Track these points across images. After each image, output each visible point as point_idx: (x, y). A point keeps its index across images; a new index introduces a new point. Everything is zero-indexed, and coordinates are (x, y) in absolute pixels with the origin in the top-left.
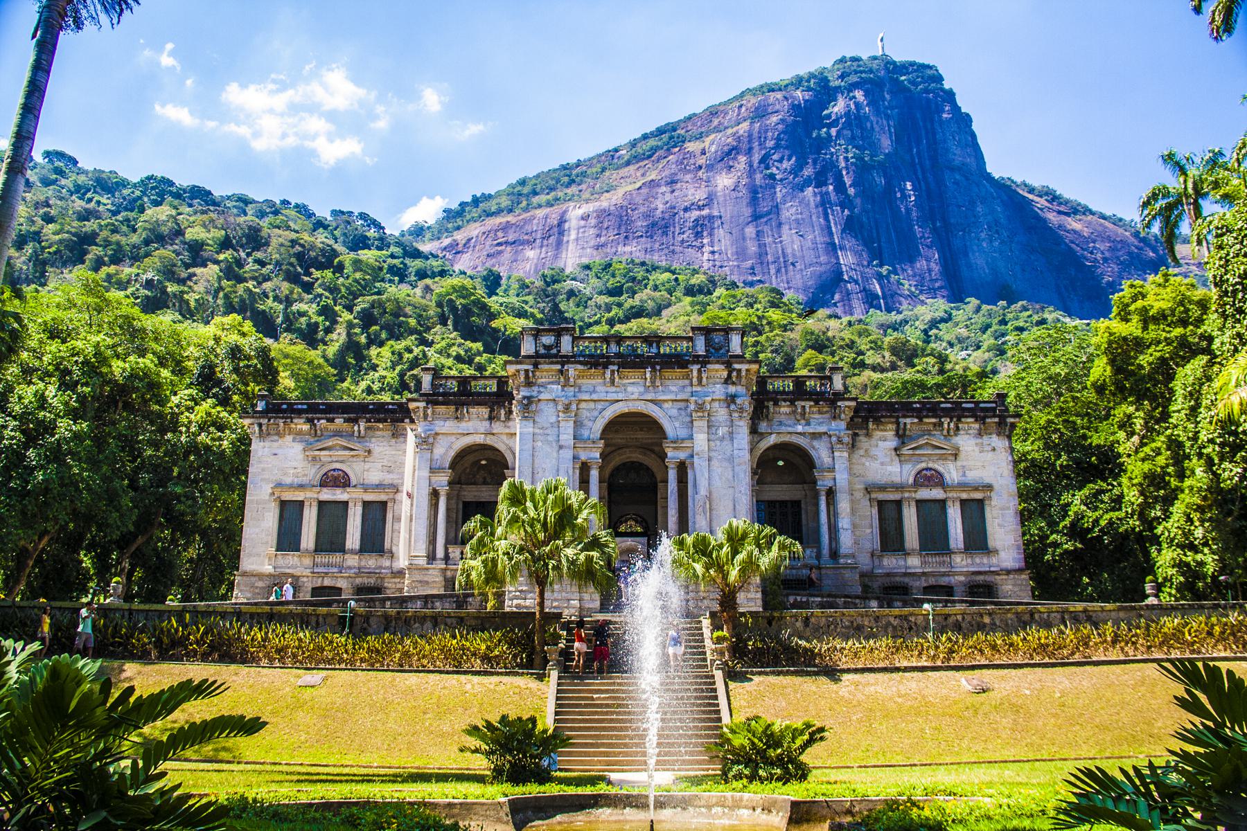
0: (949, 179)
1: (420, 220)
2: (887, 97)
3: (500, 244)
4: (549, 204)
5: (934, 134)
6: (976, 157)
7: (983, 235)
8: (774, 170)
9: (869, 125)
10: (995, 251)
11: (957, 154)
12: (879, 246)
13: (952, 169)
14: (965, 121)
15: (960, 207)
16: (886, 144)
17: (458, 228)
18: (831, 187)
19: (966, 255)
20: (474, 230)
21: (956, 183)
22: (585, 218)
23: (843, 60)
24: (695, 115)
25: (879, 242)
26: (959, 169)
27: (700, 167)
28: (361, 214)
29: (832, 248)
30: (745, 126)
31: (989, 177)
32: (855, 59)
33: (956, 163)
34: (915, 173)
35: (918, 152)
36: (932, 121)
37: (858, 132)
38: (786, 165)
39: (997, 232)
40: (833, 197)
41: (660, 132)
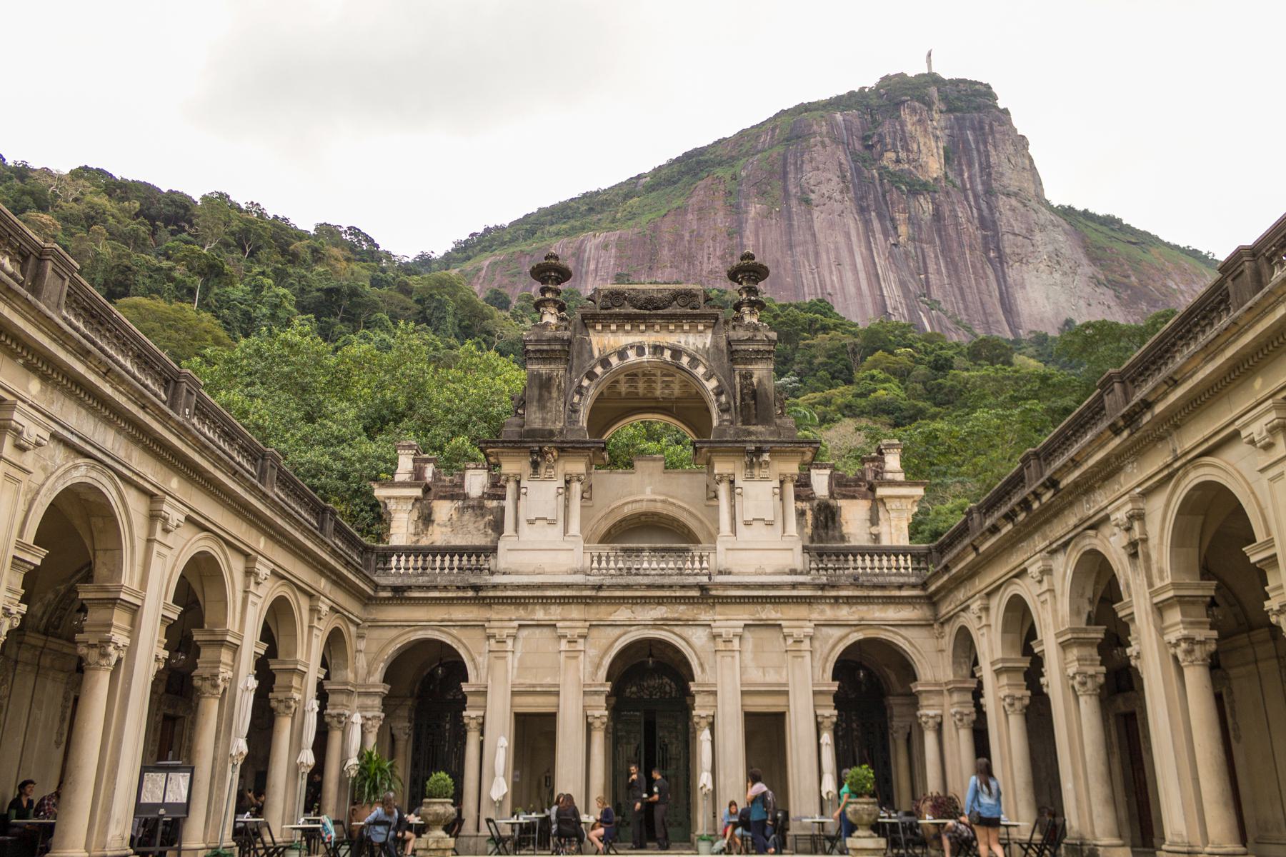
0: (1003, 203)
1: (427, 250)
2: (936, 116)
3: (514, 275)
4: (568, 234)
5: (988, 157)
6: (1034, 182)
7: (1042, 267)
8: (813, 196)
9: (915, 147)
10: (1055, 284)
11: (1011, 179)
12: (927, 278)
13: (1008, 195)
14: (1022, 142)
15: (1015, 234)
16: (934, 166)
17: (469, 258)
18: (873, 214)
19: (1023, 287)
20: (485, 261)
21: (1013, 210)
22: (606, 247)
23: (887, 78)
24: (725, 139)
25: (926, 272)
26: (1016, 195)
27: (730, 193)
28: (350, 228)
29: (874, 278)
30: (780, 149)
31: (1047, 204)
32: (902, 76)
33: (1011, 189)
34: (967, 198)
35: (970, 177)
36: (985, 143)
37: (903, 155)
38: (824, 189)
39: (1058, 263)
40: (876, 225)
41: (688, 155)
